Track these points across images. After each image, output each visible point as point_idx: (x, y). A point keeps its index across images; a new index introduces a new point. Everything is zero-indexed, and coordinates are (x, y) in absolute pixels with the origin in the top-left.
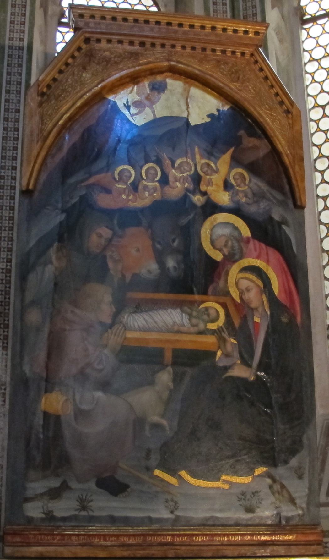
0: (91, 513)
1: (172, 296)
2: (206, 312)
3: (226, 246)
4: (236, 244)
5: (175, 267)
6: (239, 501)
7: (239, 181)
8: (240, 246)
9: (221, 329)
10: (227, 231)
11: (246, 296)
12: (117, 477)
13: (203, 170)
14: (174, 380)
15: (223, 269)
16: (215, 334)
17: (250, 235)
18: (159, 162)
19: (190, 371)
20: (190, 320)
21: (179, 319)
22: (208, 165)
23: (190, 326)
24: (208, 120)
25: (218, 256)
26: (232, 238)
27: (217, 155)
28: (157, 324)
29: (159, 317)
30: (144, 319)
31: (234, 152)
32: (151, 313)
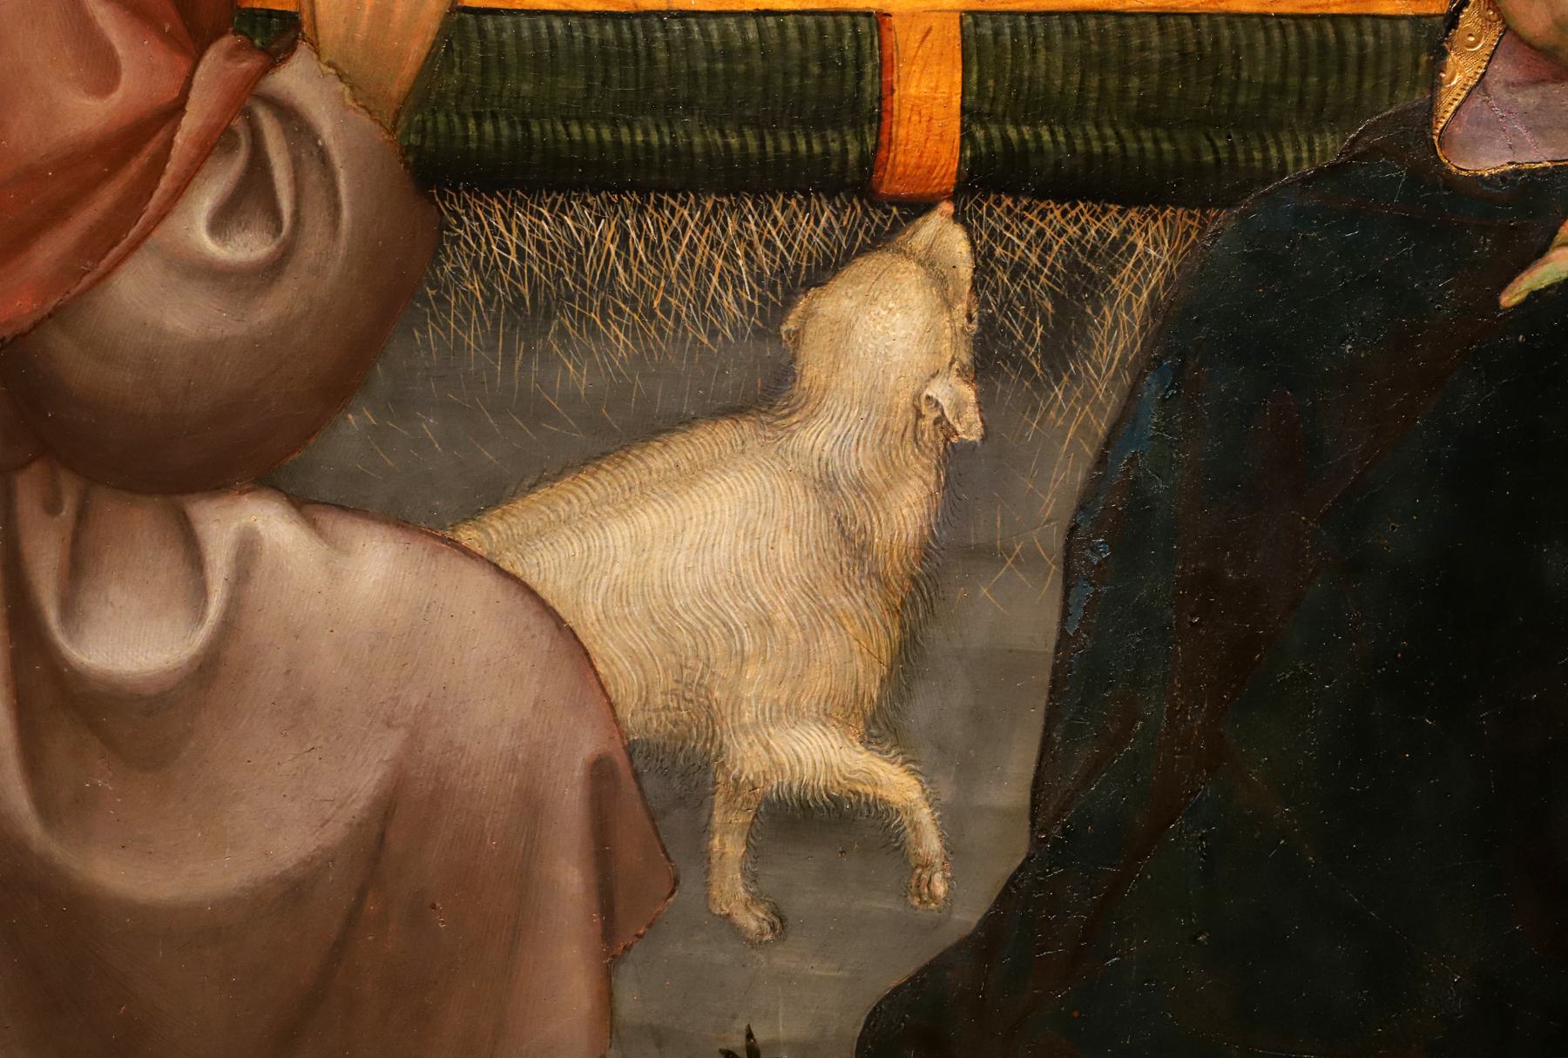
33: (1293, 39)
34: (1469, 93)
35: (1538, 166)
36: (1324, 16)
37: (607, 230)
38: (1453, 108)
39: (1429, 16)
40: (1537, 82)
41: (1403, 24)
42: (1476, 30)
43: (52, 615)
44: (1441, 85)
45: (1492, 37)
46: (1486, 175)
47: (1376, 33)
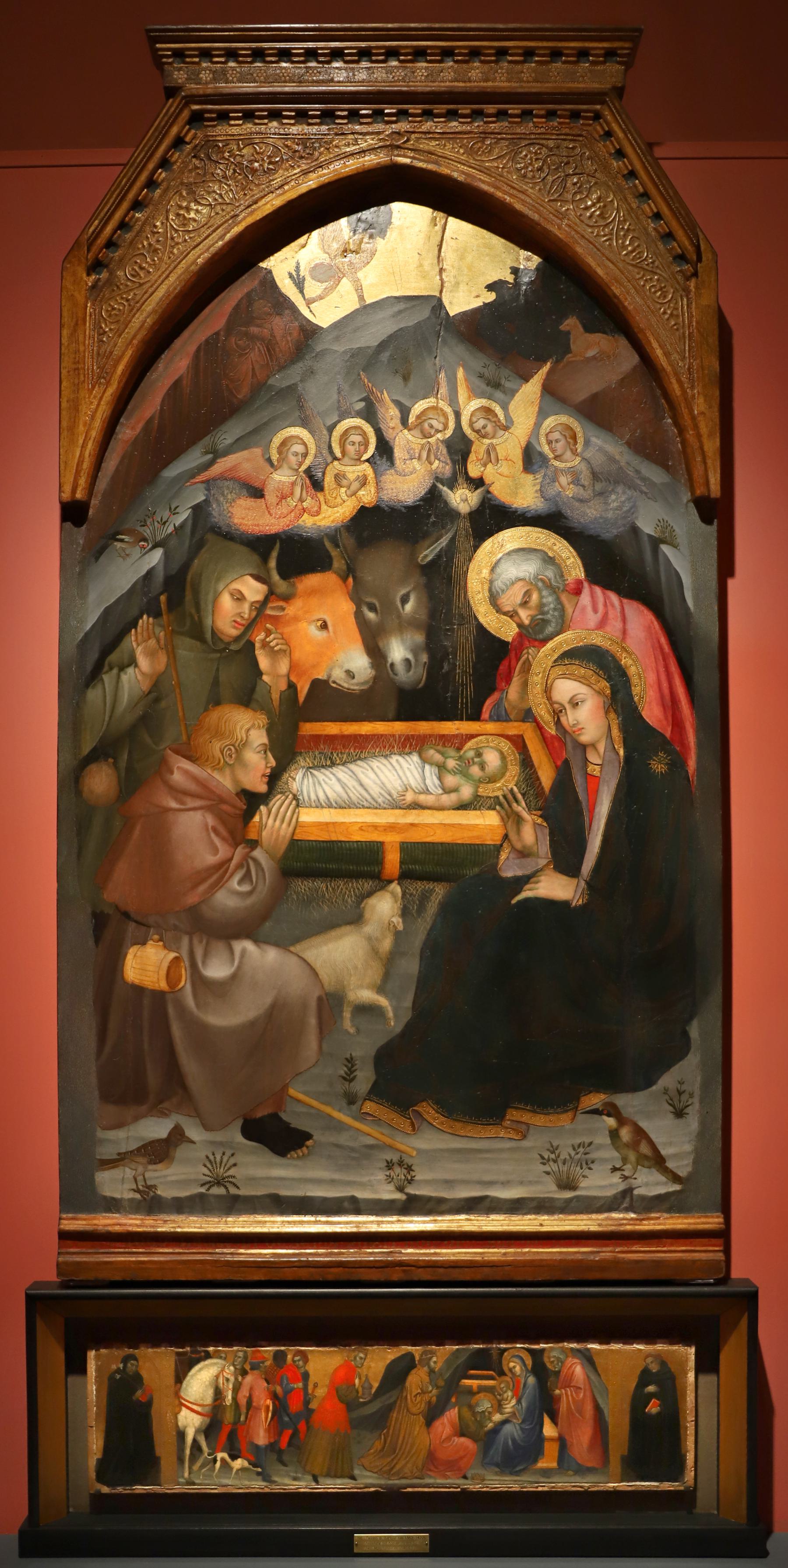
0: (233, 1191)
1: (399, 728)
2: (476, 760)
3: (524, 604)
4: (550, 599)
5: (407, 661)
6: (544, 1164)
7: (560, 446)
8: (558, 600)
9: (510, 797)
10: (528, 568)
11: (570, 718)
12: (284, 1116)
13: (475, 425)
14: (405, 913)
15: (518, 660)
16: (498, 807)
17: (582, 575)
18: (370, 414)
19: (439, 891)
20: (440, 778)
21: (417, 776)
22: (488, 411)
23: (441, 791)
24: (491, 297)
25: (507, 631)
26: (540, 584)
27: (508, 385)
28: (366, 790)
29: (372, 775)
30: (339, 780)
31: (549, 373)
32: (352, 766)
37: (323, 886)
43: (200, 965)
45: (509, 849)
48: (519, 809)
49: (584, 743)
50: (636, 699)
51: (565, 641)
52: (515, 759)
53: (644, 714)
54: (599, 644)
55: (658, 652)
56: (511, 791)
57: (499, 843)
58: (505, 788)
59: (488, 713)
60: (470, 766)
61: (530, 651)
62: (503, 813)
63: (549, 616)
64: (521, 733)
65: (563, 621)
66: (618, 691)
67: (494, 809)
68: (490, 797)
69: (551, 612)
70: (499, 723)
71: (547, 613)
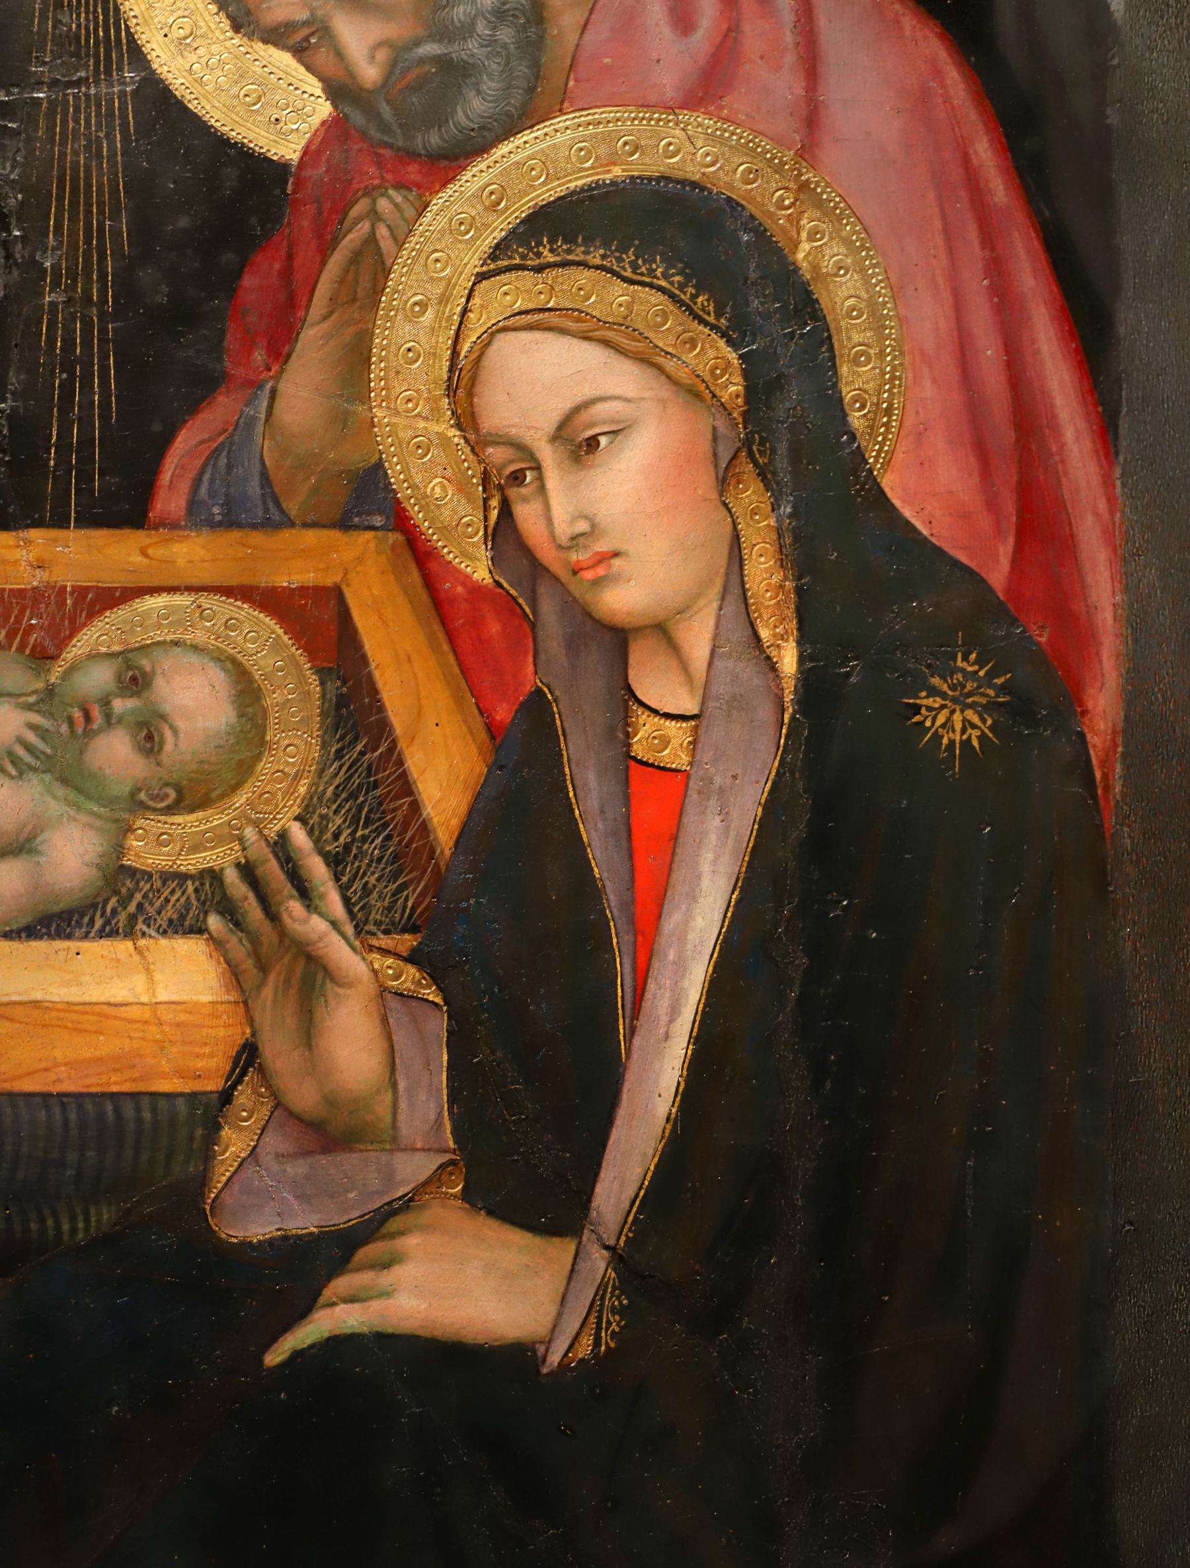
2: (120, 705)
9: (272, 870)
16: (214, 922)
33: (73, 1116)
34: (241, 1165)
35: (304, 1231)
36: (103, 1095)
38: (224, 1179)
39: (205, 1093)
40: (306, 1153)
41: (181, 1100)
42: (249, 1105)
44: (214, 1157)
45: (265, 1112)
46: (255, 1241)
47: (154, 1110)
48: (318, 924)
49: (621, 620)
50: (856, 419)
51: (545, 159)
52: (308, 694)
53: (887, 483)
54: (693, 172)
55: (961, 204)
56: (281, 846)
57: (214, 1085)
58: (250, 833)
59: (184, 487)
60: (89, 734)
61: (383, 204)
62: (238, 947)
63: (472, 45)
64: (329, 580)
65: (537, 73)
66: (778, 384)
67: (198, 930)
68: (183, 877)
69: (481, 28)
70: (235, 535)
71: (467, 30)
